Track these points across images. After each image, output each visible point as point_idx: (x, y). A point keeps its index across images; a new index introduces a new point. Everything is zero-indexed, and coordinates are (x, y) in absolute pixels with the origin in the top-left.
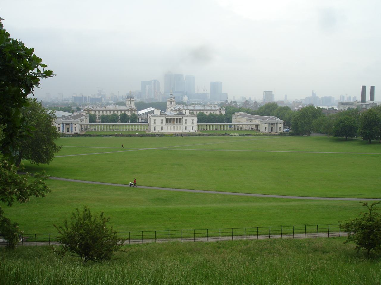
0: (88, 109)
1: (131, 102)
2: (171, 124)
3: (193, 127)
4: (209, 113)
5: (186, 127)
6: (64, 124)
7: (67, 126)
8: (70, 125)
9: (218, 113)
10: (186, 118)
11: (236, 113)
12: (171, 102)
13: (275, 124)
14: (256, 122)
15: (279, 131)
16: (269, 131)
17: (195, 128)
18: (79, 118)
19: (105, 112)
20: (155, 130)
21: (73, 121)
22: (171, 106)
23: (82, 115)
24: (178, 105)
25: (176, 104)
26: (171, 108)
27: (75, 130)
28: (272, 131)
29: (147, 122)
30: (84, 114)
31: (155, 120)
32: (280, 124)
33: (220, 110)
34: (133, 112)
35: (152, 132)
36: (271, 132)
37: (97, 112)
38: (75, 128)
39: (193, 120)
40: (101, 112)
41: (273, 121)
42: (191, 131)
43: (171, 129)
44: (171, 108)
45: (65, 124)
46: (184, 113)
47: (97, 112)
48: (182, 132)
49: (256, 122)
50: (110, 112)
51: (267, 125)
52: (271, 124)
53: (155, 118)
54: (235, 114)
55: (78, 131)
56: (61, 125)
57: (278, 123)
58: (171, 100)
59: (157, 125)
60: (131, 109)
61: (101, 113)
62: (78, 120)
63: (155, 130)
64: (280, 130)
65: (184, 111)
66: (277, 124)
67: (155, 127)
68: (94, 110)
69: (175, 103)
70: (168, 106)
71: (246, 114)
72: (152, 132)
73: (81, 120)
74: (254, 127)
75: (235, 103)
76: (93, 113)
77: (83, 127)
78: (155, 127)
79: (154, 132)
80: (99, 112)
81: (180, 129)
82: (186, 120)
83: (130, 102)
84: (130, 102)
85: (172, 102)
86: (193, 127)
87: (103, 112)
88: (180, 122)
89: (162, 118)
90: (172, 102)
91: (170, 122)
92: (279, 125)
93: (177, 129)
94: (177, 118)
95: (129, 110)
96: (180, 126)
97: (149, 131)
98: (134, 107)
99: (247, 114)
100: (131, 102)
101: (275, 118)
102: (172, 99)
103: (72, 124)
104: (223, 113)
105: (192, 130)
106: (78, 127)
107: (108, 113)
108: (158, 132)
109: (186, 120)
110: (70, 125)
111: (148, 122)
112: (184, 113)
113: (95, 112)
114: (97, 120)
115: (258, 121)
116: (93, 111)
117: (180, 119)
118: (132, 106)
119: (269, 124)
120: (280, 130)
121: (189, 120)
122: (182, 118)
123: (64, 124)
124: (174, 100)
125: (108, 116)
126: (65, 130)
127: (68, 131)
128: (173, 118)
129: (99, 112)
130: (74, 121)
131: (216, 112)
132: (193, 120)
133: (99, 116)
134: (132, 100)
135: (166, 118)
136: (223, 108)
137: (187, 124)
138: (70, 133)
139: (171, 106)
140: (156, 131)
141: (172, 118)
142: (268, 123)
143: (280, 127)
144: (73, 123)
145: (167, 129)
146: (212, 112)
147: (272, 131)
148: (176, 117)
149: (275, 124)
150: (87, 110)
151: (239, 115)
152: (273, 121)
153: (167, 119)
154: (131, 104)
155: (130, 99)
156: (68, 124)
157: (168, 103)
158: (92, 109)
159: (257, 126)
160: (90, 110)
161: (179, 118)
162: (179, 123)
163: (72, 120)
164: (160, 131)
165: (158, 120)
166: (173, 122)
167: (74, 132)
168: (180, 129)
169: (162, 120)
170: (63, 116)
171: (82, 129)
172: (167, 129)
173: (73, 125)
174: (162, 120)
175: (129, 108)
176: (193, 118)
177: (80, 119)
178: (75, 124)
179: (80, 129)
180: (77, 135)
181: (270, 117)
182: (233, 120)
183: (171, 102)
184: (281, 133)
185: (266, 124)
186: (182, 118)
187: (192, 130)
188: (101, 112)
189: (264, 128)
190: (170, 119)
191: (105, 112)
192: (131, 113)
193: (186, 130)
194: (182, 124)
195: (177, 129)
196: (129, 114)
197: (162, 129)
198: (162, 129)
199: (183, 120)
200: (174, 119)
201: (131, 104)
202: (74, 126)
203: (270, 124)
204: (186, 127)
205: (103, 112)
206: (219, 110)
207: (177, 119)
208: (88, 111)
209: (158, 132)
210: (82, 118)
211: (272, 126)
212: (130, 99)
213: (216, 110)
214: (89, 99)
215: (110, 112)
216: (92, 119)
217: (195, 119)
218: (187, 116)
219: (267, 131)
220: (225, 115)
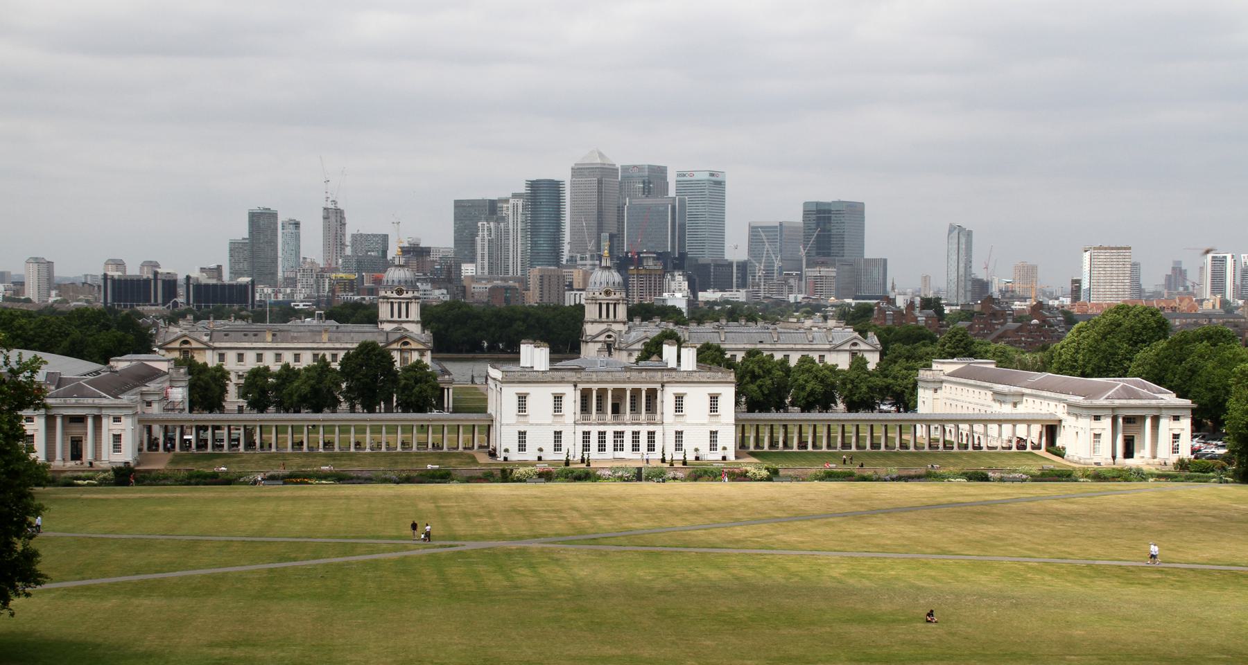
0: (186, 342)
1: (403, 306)
2: (602, 416)
3: (714, 434)
4: (794, 360)
5: (679, 434)
6: (59, 421)
7: (75, 430)
8: (90, 421)
9: (842, 362)
10: (680, 389)
11: (934, 366)
12: (604, 307)
13: (1148, 422)
14: (1040, 404)
15: (1166, 456)
16: (1114, 457)
17: (728, 438)
18: (137, 390)
20: (522, 447)
21: (105, 401)
22: (604, 326)
23: (155, 374)
24: (637, 321)
25: (630, 316)
26: (602, 338)
28: (1129, 453)
29: (484, 410)
30: (163, 366)
32: (1176, 418)
33: (855, 344)
34: (415, 357)
35: (506, 459)
36: (1129, 462)
37: (231, 357)
38: (117, 438)
39: (714, 399)
40: (250, 358)
41: (1133, 402)
43: (602, 447)
44: (602, 338)
45: (64, 417)
46: (672, 363)
47: (231, 357)
50: (297, 358)
51: (1106, 423)
52: (1128, 420)
53: (523, 389)
54: (928, 367)
55: (127, 455)
57: (1164, 412)
58: (603, 296)
60: (404, 340)
61: (250, 362)
62: (125, 399)
63: (522, 447)
64: (1175, 450)
65: (669, 351)
66: (1156, 419)
67: (522, 435)
68: (215, 349)
69: (622, 312)
70: (590, 329)
71: (990, 365)
72: (506, 459)
73: (149, 398)
74: (1034, 434)
75: (931, 312)
77: (158, 432)
78: (522, 435)
79: (515, 456)
80: (240, 358)
81: (651, 447)
82: (679, 398)
83: (396, 306)
84: (396, 306)
85: (611, 307)
86: (714, 434)
87: (260, 358)
88: (651, 408)
89: (558, 389)
90: (611, 307)
91: (600, 409)
92: (1166, 425)
93: (636, 447)
94: (633, 390)
95: (394, 346)
96: (651, 428)
97: (493, 454)
99: (993, 366)
100: (403, 306)
101: (1145, 387)
102: (607, 293)
103: (98, 419)
104: (873, 361)
105: (713, 446)
106: (127, 428)
108: (540, 459)
109: (679, 398)
110: (90, 421)
111: (489, 411)
112: (672, 363)
113: (222, 357)
114: (232, 398)
115: (1052, 404)
116: (209, 353)
117: (652, 395)
118: (404, 325)
119: (1115, 419)
120: (1175, 450)
121: (697, 397)
122: (658, 386)
123: (59, 421)
124: (618, 296)
125: (288, 374)
127: (77, 454)
128: (614, 390)
129: (240, 358)
130: (109, 400)
131: (834, 355)
132: (714, 399)
133: (240, 377)
134: (410, 295)
135: (580, 386)
136: (870, 334)
137: (688, 419)
139: (604, 326)
140: (530, 455)
141: (610, 387)
142: (1110, 412)
143: (1176, 437)
144: (104, 412)
145: (586, 446)
147: (1129, 453)
148: (629, 381)
149: (1148, 422)
150: (177, 345)
151: (949, 375)
152: (1133, 402)
153: (585, 396)
154: (404, 318)
155: (400, 292)
156: (81, 419)
157: (591, 312)
158: (206, 339)
159: (1051, 431)
160: (195, 345)
161: (644, 387)
162: (643, 415)
163: (101, 397)
164: (550, 455)
165: (540, 397)
166: (616, 409)
167: (111, 458)
168: (651, 447)
169: (558, 398)
171: (153, 445)
172: (586, 446)
173: (107, 424)
174: (558, 398)
175: (393, 337)
176: (715, 389)
177: (142, 394)
178: (117, 419)
179: (142, 443)
180: (123, 476)
181: (1119, 383)
183: (604, 307)
184: (1182, 465)
185: (1097, 418)
186: (658, 386)
188: (250, 358)
189: (1087, 442)
190: (602, 394)
192: (404, 360)
193: (679, 446)
194: (658, 417)
195: (636, 447)
197: (558, 447)
198: (558, 447)
199: (667, 399)
200: (619, 394)
201: (404, 318)
202: (108, 425)
203: (1120, 420)
204: (679, 434)
205: (260, 358)
206: (847, 347)
207: (636, 394)
208: (185, 352)
209: (540, 459)
210: (152, 386)
212: (400, 292)
213: (835, 349)
214: (109, 282)
215: (297, 358)
217: (727, 394)
218: (688, 380)
220: (882, 369)
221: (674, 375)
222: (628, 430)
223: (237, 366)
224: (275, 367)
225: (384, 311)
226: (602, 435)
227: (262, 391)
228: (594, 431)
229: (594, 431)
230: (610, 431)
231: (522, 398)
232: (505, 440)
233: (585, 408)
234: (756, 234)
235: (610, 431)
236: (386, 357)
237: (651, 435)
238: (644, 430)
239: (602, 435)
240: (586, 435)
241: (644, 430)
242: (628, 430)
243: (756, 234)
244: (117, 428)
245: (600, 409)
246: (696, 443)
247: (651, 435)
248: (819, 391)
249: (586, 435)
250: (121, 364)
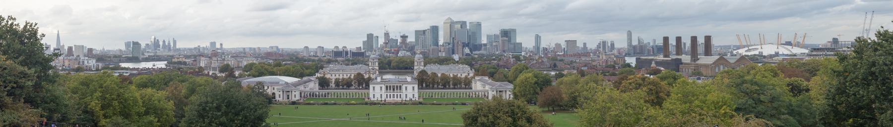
17: (416, 96)
49: (487, 87)
56: (281, 93)
59: (377, 92)
61: (337, 76)
76: (328, 76)
106: (298, 94)
114: (333, 85)
121: (410, 87)
125: (343, 79)
126: (285, 97)
165: (377, 87)
167: (294, 99)
170: (287, 83)
180: (294, 103)
182: (473, 85)
196: (366, 76)
199: (404, 87)
216: (324, 83)
217: (416, 86)
221: (406, 82)
223: (333, 78)
224: (341, 77)
227: (338, 83)
232: (371, 96)
234: (488, 37)
236: (362, 76)
243: (488, 37)
246: (410, 96)
248: (445, 82)
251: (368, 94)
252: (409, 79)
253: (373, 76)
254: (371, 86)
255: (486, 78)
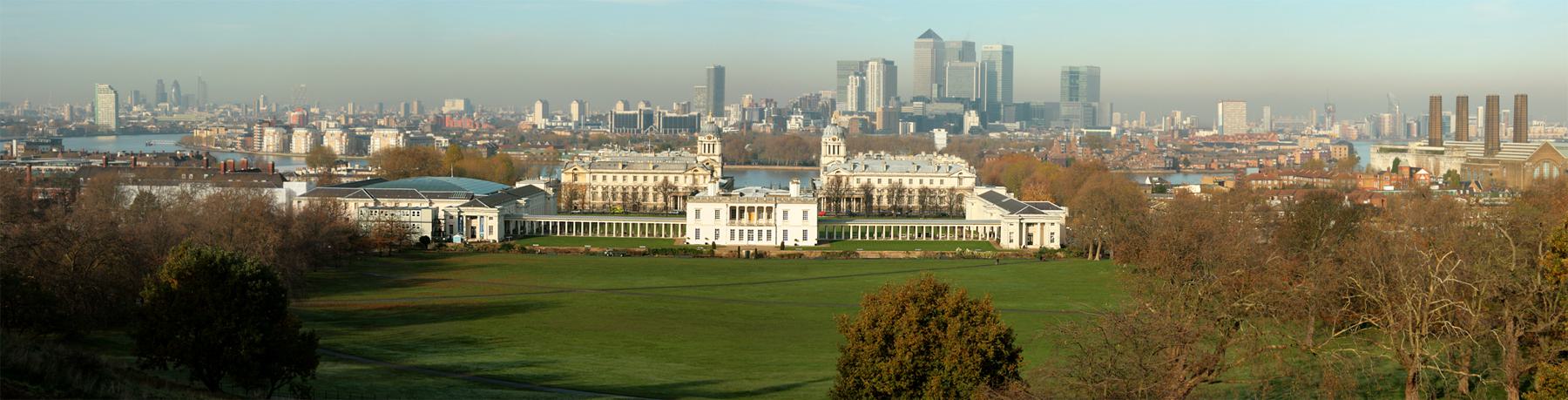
5: (785, 232)
19: (620, 177)
20: (697, 237)
27: (491, 232)
28: (1030, 243)
30: (541, 186)
31: (698, 212)
37: (599, 177)
38: (491, 228)
39: (805, 213)
40: (610, 177)
42: (802, 243)
47: (599, 177)
48: (772, 243)
51: (1017, 226)
59: (707, 224)
63: (697, 237)
67: (697, 231)
70: (824, 160)
76: (585, 179)
78: (697, 231)
79: (693, 242)
82: (785, 213)
98: (718, 159)
105: (805, 238)
107: (630, 181)
109: (785, 213)
117: (770, 210)
121: (796, 210)
132: (805, 213)
138: (478, 238)
140: (702, 242)
145: (732, 237)
146: (937, 184)
153: (733, 210)
157: (824, 150)
165: (708, 209)
174: (717, 212)
187: (805, 238)
188: (610, 177)
191: (620, 177)
192: (695, 181)
196: (684, 183)
197: (717, 236)
198: (717, 236)
200: (751, 209)
204: (785, 232)
207: (760, 209)
208: (575, 176)
211: (1031, 229)
217: (813, 210)
218: (791, 201)
219: (1015, 245)
222: (756, 230)
225: (700, 148)
226: (741, 232)
228: (737, 229)
229: (737, 229)
230: (746, 229)
231: (698, 212)
232: (690, 233)
233: (733, 216)
235: (746, 229)
237: (769, 232)
238: (765, 230)
239: (741, 232)
240: (732, 231)
241: (765, 230)
242: (756, 230)
244: (490, 223)
245: (741, 217)
247: (769, 232)
249: (732, 231)
250: (518, 185)
251: (684, 227)
252: (794, 189)
253: (701, 183)
254: (691, 207)
255: (1001, 191)
